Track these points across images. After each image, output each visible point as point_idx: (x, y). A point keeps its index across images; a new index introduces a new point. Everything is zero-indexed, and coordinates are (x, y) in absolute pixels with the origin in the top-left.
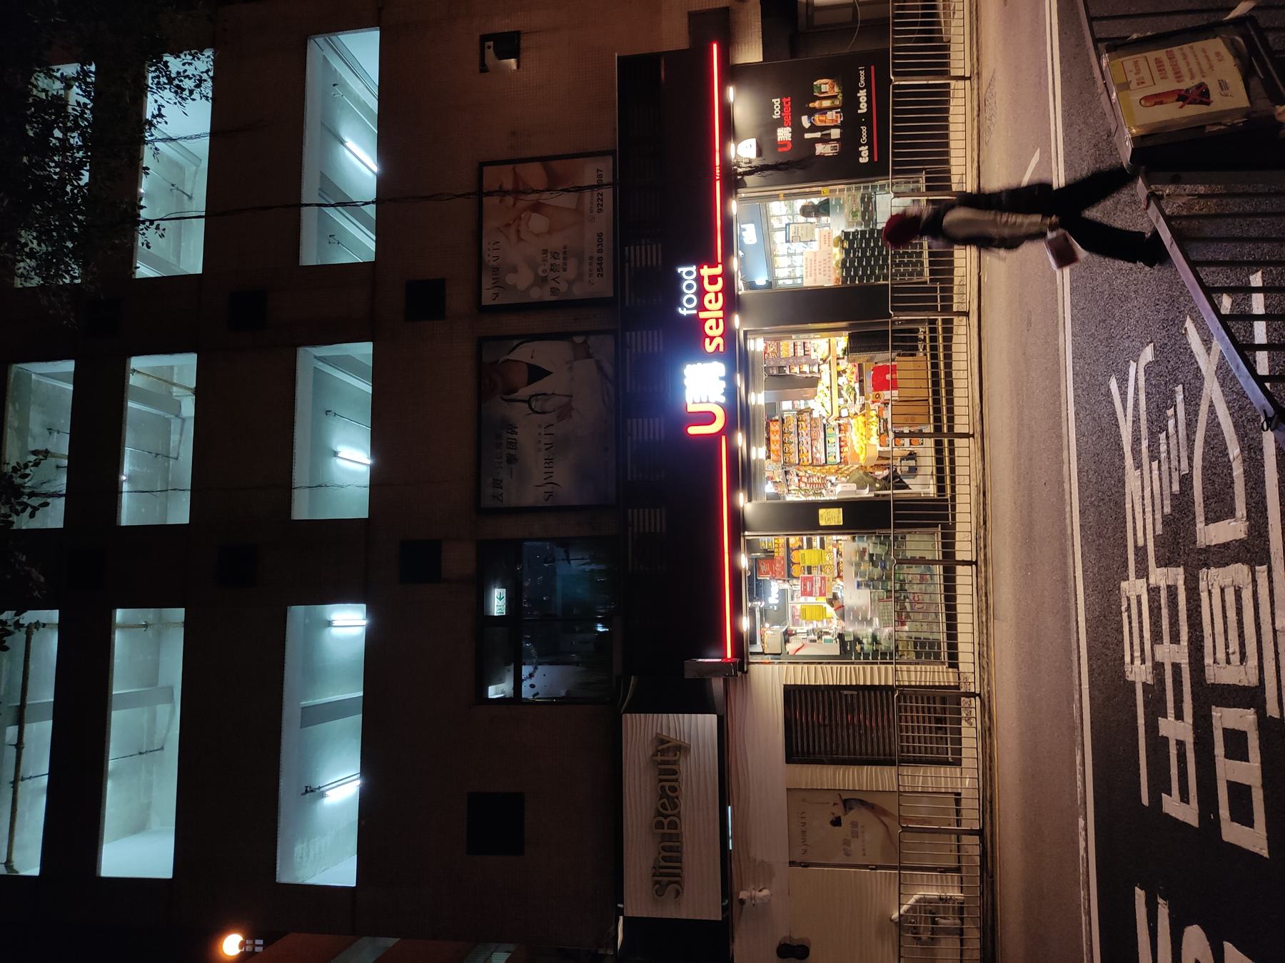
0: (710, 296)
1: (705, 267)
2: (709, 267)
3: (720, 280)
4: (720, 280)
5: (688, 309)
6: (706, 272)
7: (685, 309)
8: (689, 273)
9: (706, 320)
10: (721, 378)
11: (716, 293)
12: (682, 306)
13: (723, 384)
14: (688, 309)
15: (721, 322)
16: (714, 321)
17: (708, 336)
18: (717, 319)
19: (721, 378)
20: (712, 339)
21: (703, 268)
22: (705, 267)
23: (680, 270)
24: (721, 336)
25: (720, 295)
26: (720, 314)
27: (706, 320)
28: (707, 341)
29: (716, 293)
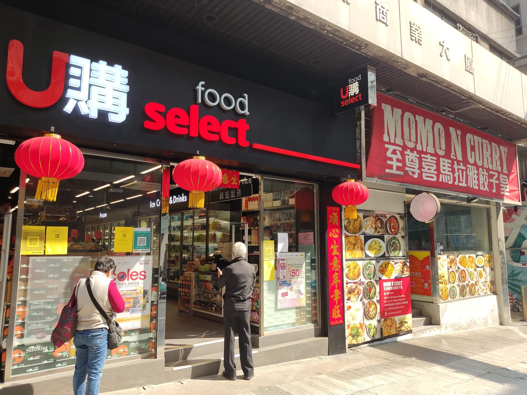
5: (203, 93)
7: (203, 89)
12: (206, 87)
13: (94, 115)
14: (203, 93)
19: (103, 114)
23: (246, 95)
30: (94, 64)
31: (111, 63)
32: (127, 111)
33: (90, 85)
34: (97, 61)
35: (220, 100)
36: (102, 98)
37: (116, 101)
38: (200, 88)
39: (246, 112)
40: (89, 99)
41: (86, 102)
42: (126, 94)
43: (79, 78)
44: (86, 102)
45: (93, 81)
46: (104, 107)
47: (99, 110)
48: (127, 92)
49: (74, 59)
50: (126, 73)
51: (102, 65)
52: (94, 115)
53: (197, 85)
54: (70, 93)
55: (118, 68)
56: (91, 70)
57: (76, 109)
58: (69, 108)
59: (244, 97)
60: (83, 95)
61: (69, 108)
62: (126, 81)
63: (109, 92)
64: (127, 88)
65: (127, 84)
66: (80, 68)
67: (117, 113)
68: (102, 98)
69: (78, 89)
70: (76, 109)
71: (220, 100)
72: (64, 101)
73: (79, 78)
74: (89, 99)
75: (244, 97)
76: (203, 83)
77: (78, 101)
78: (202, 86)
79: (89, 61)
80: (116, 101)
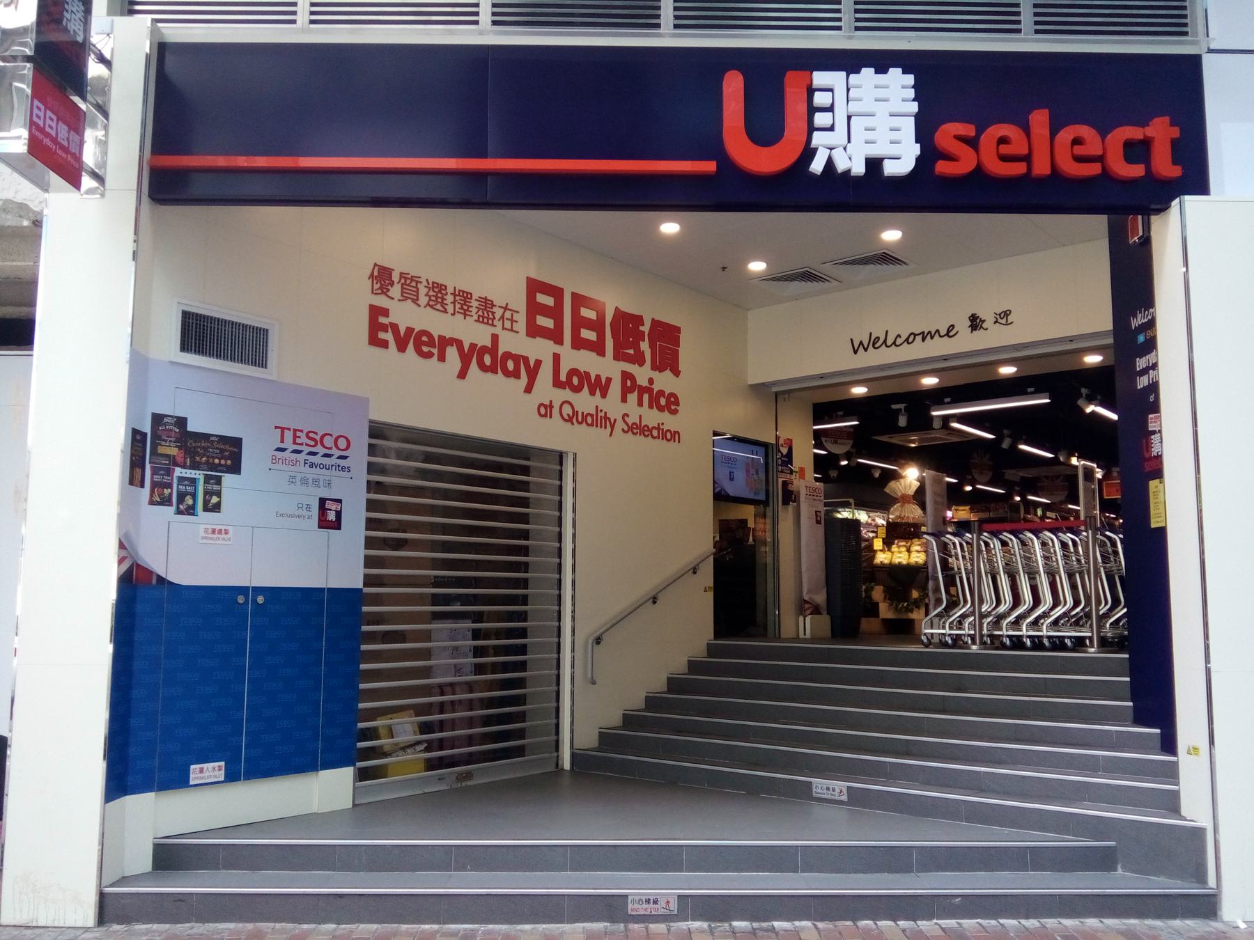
0: (1093, 145)
1: (1175, 132)
2: (1174, 143)
3: (1137, 171)
4: (1137, 171)
11: (1100, 159)
13: (859, 169)
15: (1019, 169)
16: (1024, 151)
17: (980, 131)
18: (1027, 159)
19: (874, 164)
20: (972, 142)
21: (1172, 124)
22: (1175, 132)
24: (979, 170)
25: (1094, 169)
26: (1041, 167)
27: (1027, 131)
28: (968, 130)
30: (852, 76)
32: (916, 150)
33: (849, 118)
34: (858, 72)
36: (870, 136)
37: (895, 136)
40: (849, 142)
41: (845, 149)
42: (913, 118)
43: (830, 109)
44: (845, 149)
45: (854, 107)
46: (875, 151)
47: (866, 159)
48: (914, 114)
49: (820, 78)
50: (910, 79)
52: (859, 169)
54: (818, 139)
55: (895, 73)
56: (848, 90)
57: (830, 164)
58: (817, 166)
60: (838, 137)
61: (817, 166)
62: (911, 93)
63: (882, 122)
64: (914, 107)
65: (914, 100)
66: (831, 90)
67: (899, 159)
68: (870, 136)
69: (831, 128)
70: (830, 164)
72: (809, 153)
73: (830, 109)
74: (849, 142)
77: (831, 149)
79: (844, 74)
80: (895, 136)
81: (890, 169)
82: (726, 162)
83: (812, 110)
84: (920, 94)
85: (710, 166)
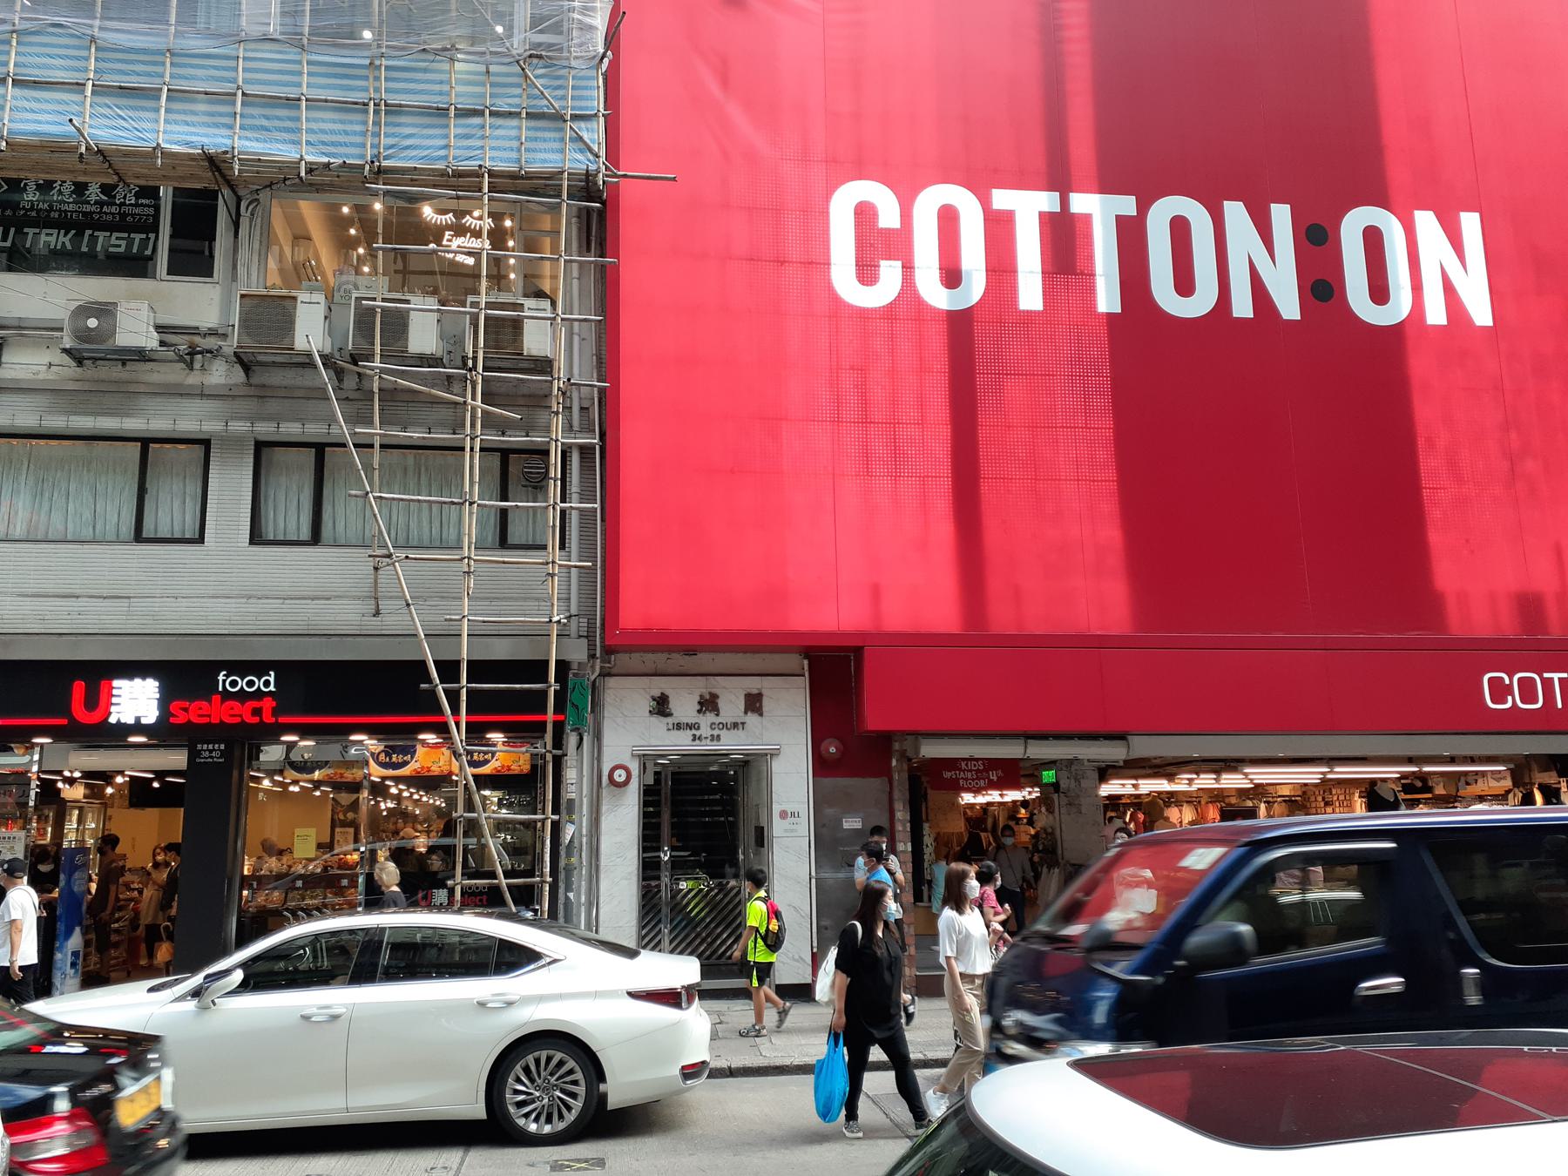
4: (256, 720)
5: (224, 681)
6: (268, 704)
8: (267, 684)
9: (210, 702)
10: (138, 719)
13: (131, 721)
14: (224, 681)
15: (206, 720)
19: (138, 719)
20: (186, 710)
23: (272, 673)
25: (239, 720)
27: (210, 702)
29: (241, 716)
31: (144, 678)
35: (242, 684)
38: (221, 678)
39: (272, 688)
42: (156, 701)
50: (157, 684)
51: (138, 681)
53: (219, 675)
54: (113, 709)
57: (119, 720)
59: (270, 675)
61: (113, 720)
62: (157, 690)
64: (158, 696)
71: (242, 684)
75: (270, 675)
76: (225, 672)
78: (224, 675)
81: (144, 721)
82: (73, 720)
83: (112, 696)
84: (162, 689)
85: (64, 722)
